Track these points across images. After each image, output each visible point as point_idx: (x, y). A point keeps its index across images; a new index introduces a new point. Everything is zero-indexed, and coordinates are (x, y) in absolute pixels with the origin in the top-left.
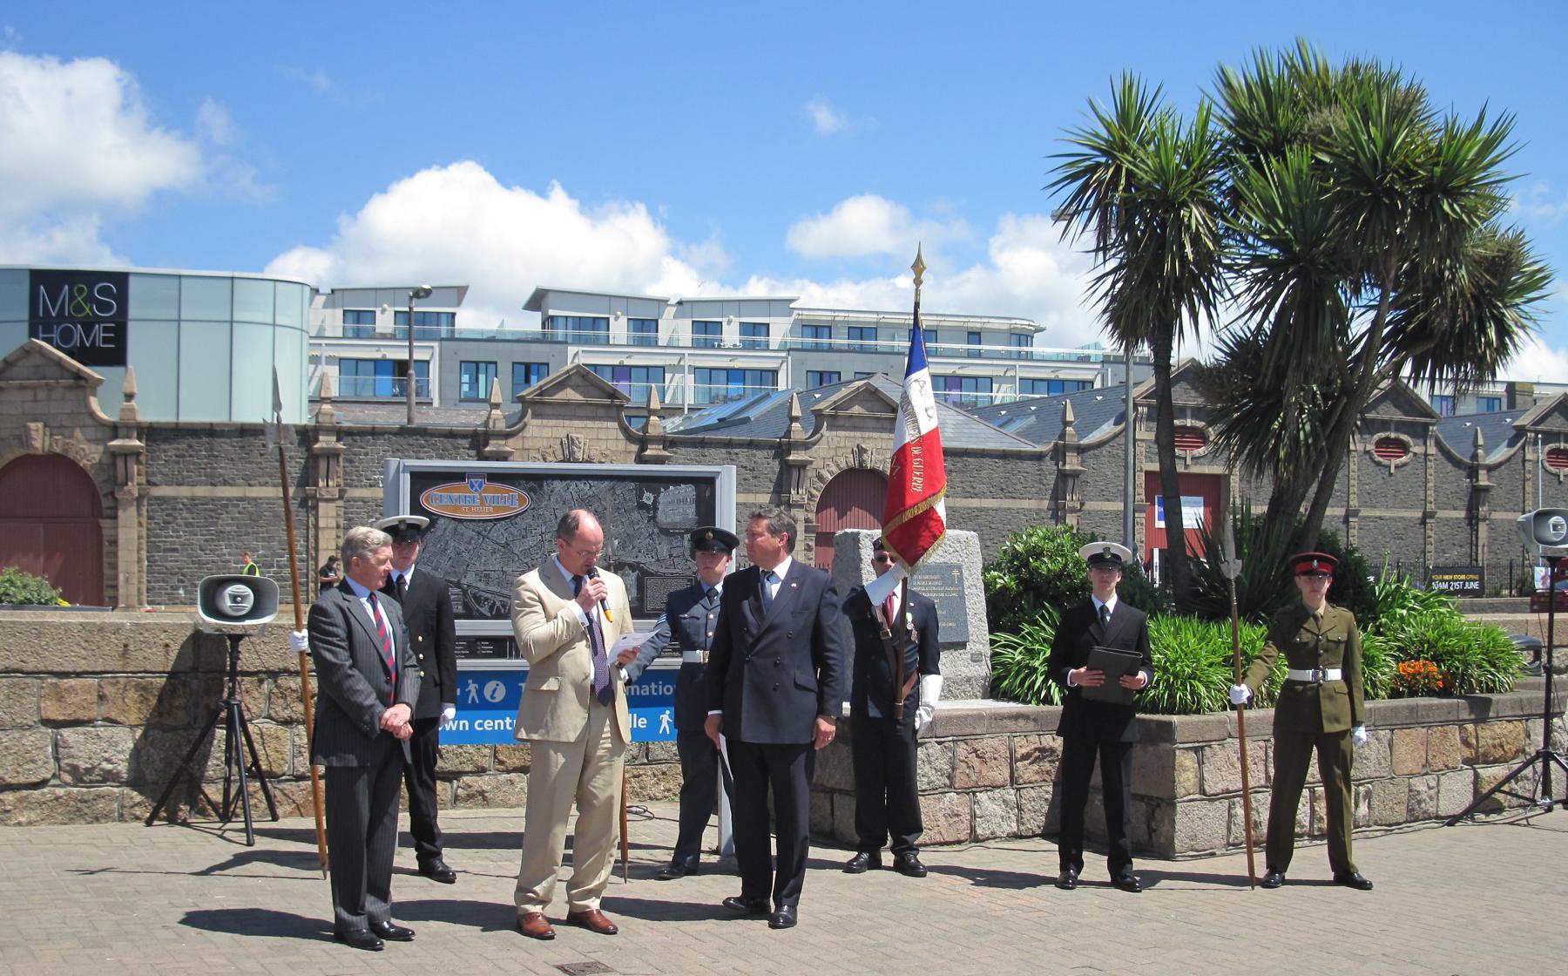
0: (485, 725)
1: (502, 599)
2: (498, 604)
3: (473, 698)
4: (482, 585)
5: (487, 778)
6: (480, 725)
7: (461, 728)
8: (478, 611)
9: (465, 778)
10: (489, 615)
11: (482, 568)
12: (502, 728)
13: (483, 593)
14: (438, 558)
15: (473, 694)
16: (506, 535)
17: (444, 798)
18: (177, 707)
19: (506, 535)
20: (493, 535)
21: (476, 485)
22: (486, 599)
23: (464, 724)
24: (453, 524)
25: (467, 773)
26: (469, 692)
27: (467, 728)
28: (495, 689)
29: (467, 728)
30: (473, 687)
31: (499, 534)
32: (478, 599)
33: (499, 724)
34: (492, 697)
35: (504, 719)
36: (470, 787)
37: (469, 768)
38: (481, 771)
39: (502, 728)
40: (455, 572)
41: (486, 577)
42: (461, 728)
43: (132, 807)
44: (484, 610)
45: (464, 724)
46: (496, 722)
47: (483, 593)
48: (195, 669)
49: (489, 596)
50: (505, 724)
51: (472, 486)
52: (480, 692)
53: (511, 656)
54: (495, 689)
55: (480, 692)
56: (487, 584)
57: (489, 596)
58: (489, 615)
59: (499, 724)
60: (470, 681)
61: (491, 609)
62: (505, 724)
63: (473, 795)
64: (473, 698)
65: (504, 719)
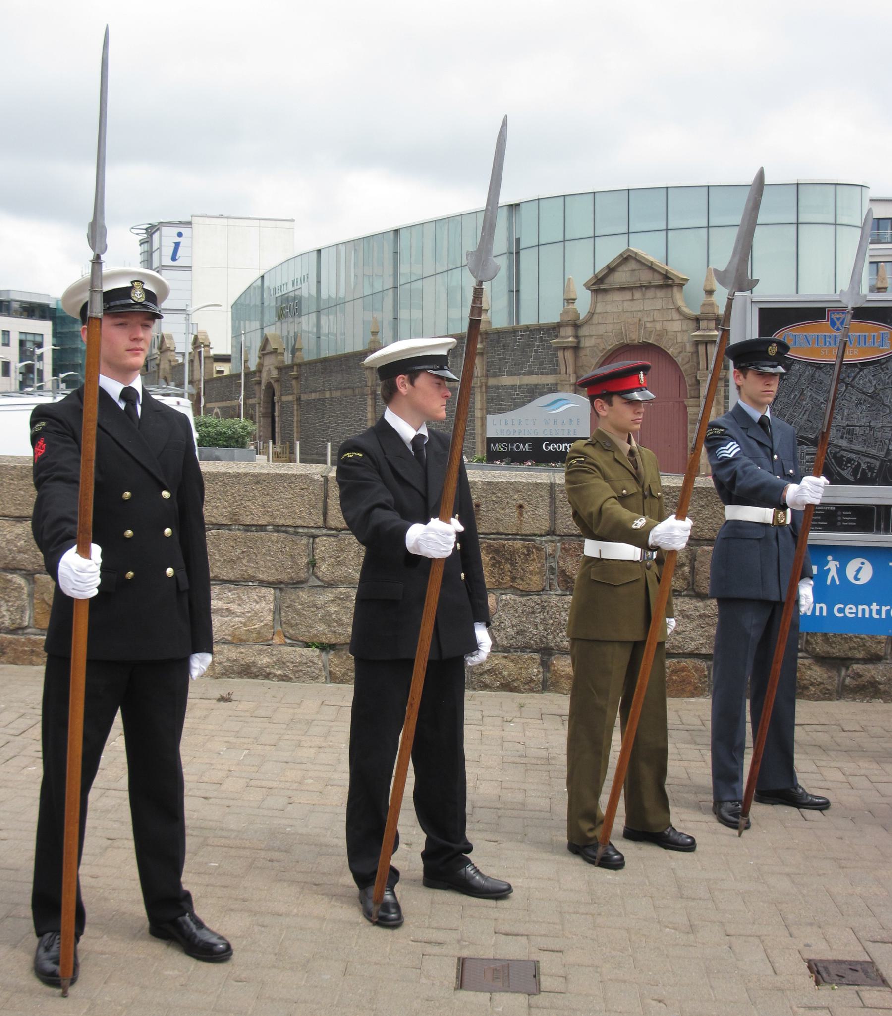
0: (847, 611)
1: (868, 460)
2: (864, 466)
3: (833, 578)
4: (844, 443)
5: (881, 667)
6: (841, 610)
7: (817, 613)
8: (839, 474)
9: (855, 666)
10: (852, 479)
11: (845, 423)
12: (867, 615)
13: (843, 453)
14: (791, 410)
15: (833, 573)
16: (874, 383)
17: (829, 687)
18: (531, 572)
19: (874, 383)
20: (860, 382)
21: (838, 323)
22: (850, 460)
23: (821, 609)
24: (809, 371)
25: (858, 661)
26: (829, 570)
27: (824, 614)
28: (860, 568)
29: (824, 614)
30: (832, 565)
31: (866, 380)
32: (840, 460)
33: (864, 610)
34: (856, 578)
35: (869, 605)
36: (860, 676)
37: (860, 655)
38: (874, 659)
39: (867, 615)
40: (812, 428)
41: (849, 433)
42: (817, 613)
43: (481, 674)
44: (847, 473)
45: (821, 609)
46: (860, 607)
47: (843, 453)
48: (551, 532)
49: (853, 456)
50: (871, 611)
51: (833, 324)
52: (841, 571)
53: (878, 530)
54: (860, 568)
55: (841, 571)
56: (851, 441)
57: (853, 456)
58: (852, 479)
59: (864, 610)
60: (830, 558)
61: (855, 472)
62: (871, 611)
63: (864, 685)
64: (833, 578)
65: (869, 605)
